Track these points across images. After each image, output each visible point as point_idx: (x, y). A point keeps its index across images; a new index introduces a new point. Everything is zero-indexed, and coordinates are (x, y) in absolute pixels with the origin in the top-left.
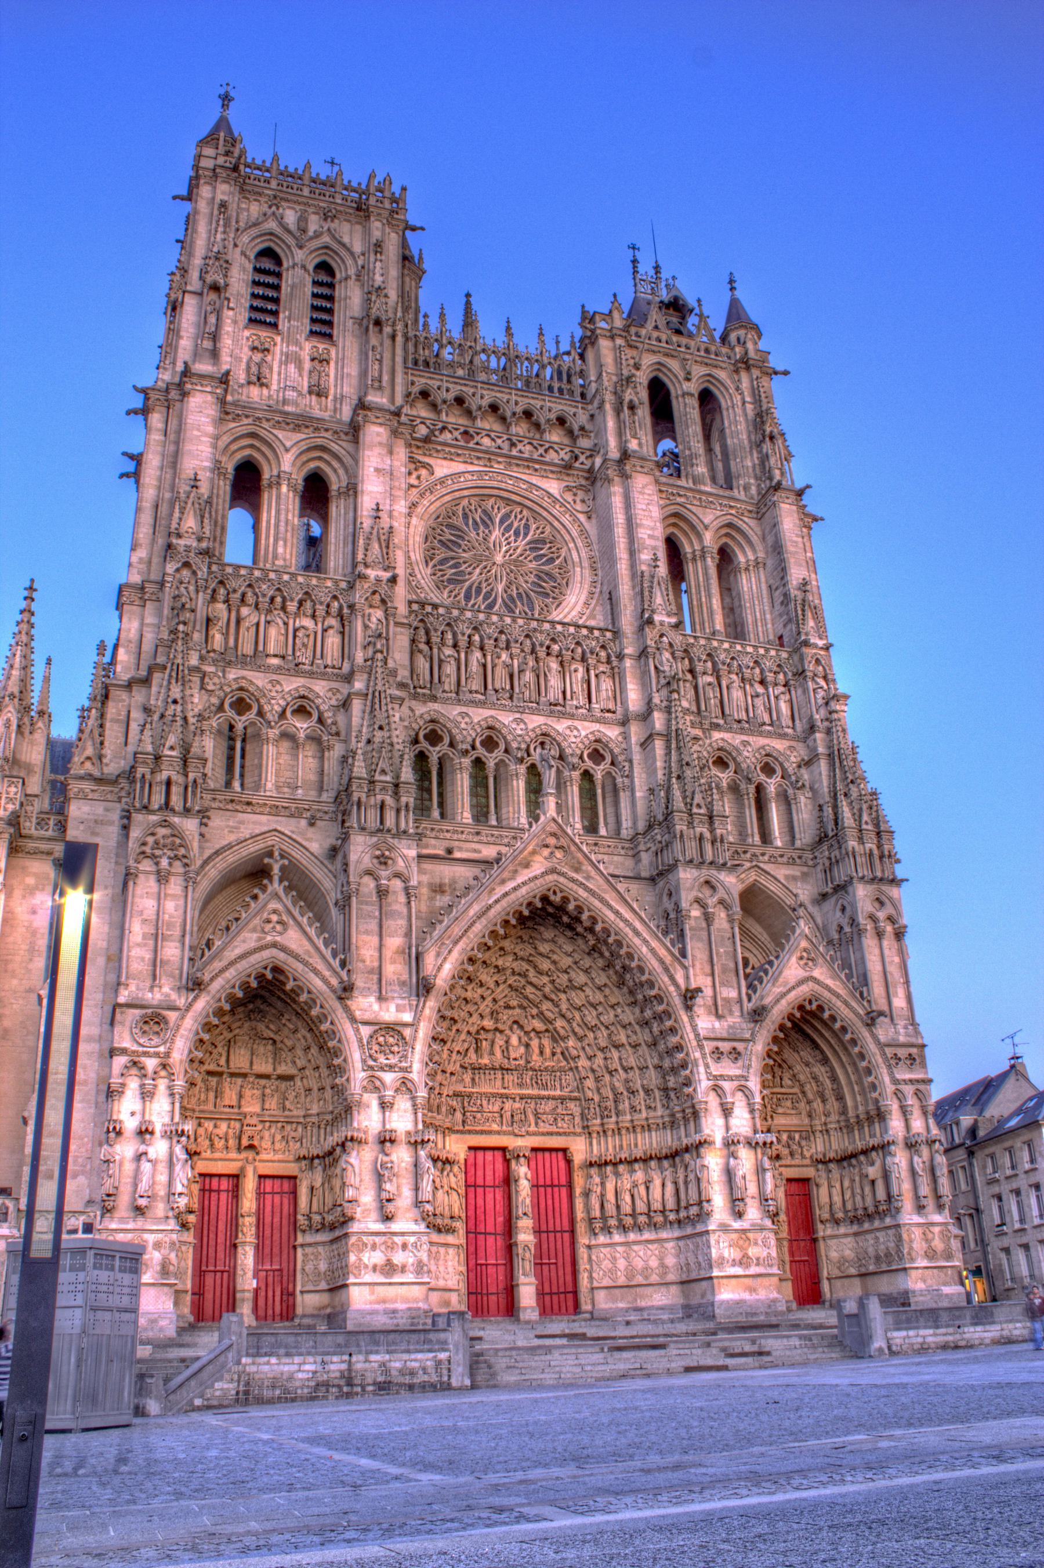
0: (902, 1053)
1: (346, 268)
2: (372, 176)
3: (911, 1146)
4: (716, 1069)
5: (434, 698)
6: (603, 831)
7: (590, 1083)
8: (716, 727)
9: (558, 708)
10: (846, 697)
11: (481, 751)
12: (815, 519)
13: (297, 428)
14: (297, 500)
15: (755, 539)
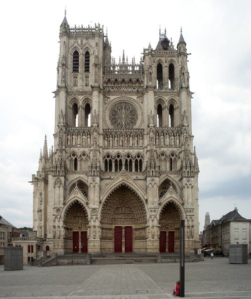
0: (189, 210)
1: (91, 52)
2: (95, 24)
3: (188, 227)
4: (151, 214)
5: (108, 149)
6: (139, 171)
7: (135, 216)
8: (162, 147)
9: (131, 148)
10: (193, 136)
11: (117, 158)
12: (193, 93)
13: (82, 95)
14: (84, 111)
15: (177, 102)
